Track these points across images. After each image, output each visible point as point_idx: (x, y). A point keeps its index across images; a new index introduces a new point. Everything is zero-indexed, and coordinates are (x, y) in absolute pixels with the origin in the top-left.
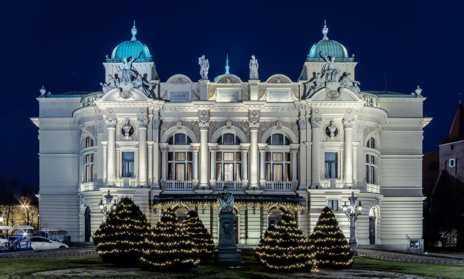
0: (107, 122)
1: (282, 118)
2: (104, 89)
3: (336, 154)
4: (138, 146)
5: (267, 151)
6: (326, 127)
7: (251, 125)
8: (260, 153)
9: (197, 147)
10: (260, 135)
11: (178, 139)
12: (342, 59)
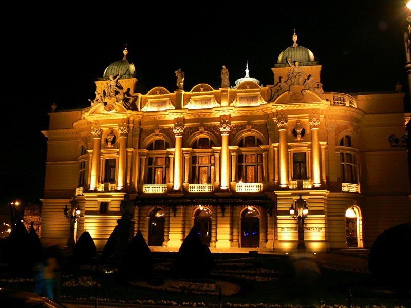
0: (93, 133)
2: (92, 103)
3: (305, 153)
4: (118, 153)
6: (293, 128)
9: (172, 152)
12: (308, 62)
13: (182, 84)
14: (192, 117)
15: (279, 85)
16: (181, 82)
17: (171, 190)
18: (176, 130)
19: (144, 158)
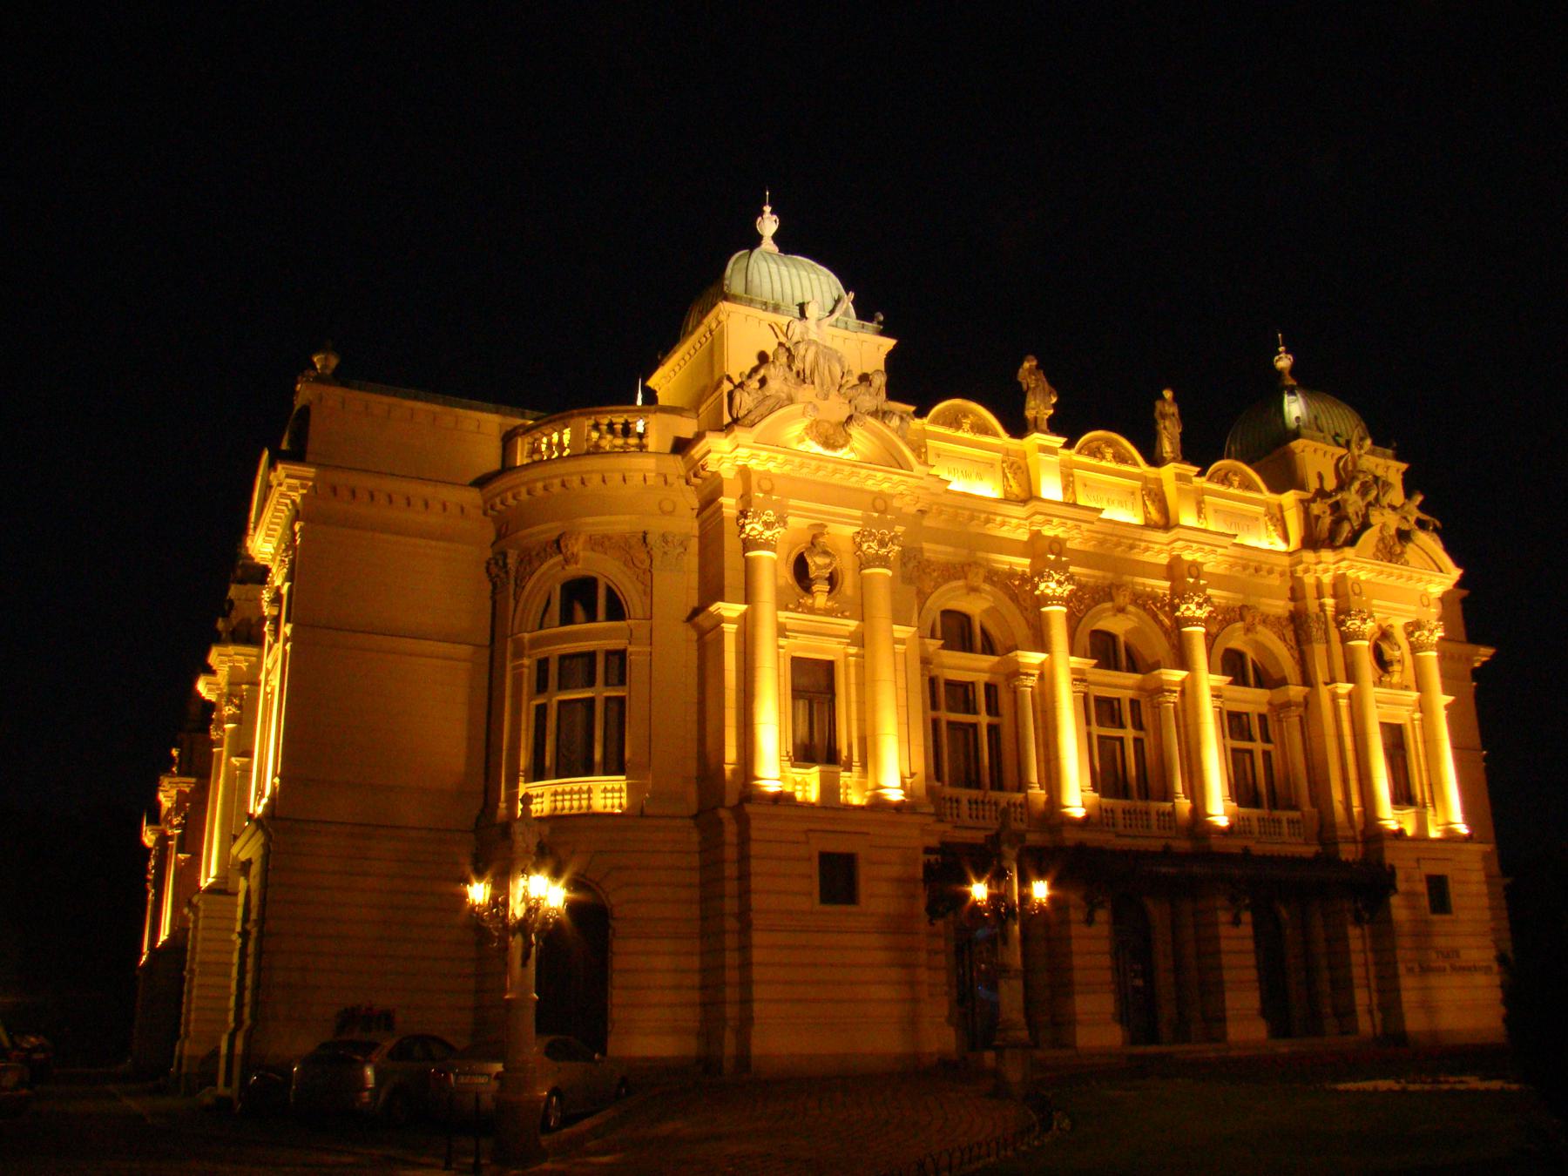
1: (1264, 600)
14: (1089, 547)
16: (1040, 406)
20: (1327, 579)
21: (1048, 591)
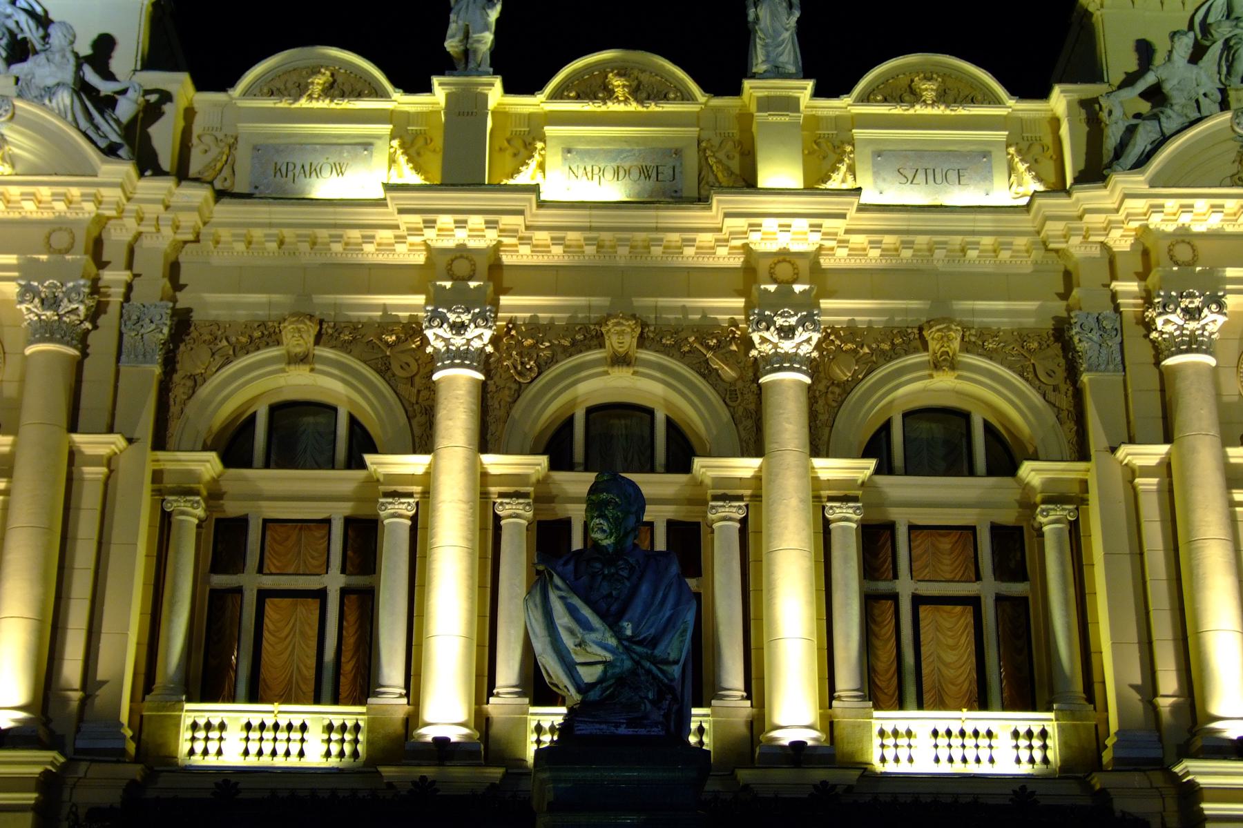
5: (876, 517)
7: (765, 342)
8: (826, 523)
10: (820, 406)
11: (297, 434)
13: (489, 37)
15: (1150, 79)
17: (402, 744)
18: (445, 332)
19: (191, 513)
20: (1121, 241)
21: (440, 345)
